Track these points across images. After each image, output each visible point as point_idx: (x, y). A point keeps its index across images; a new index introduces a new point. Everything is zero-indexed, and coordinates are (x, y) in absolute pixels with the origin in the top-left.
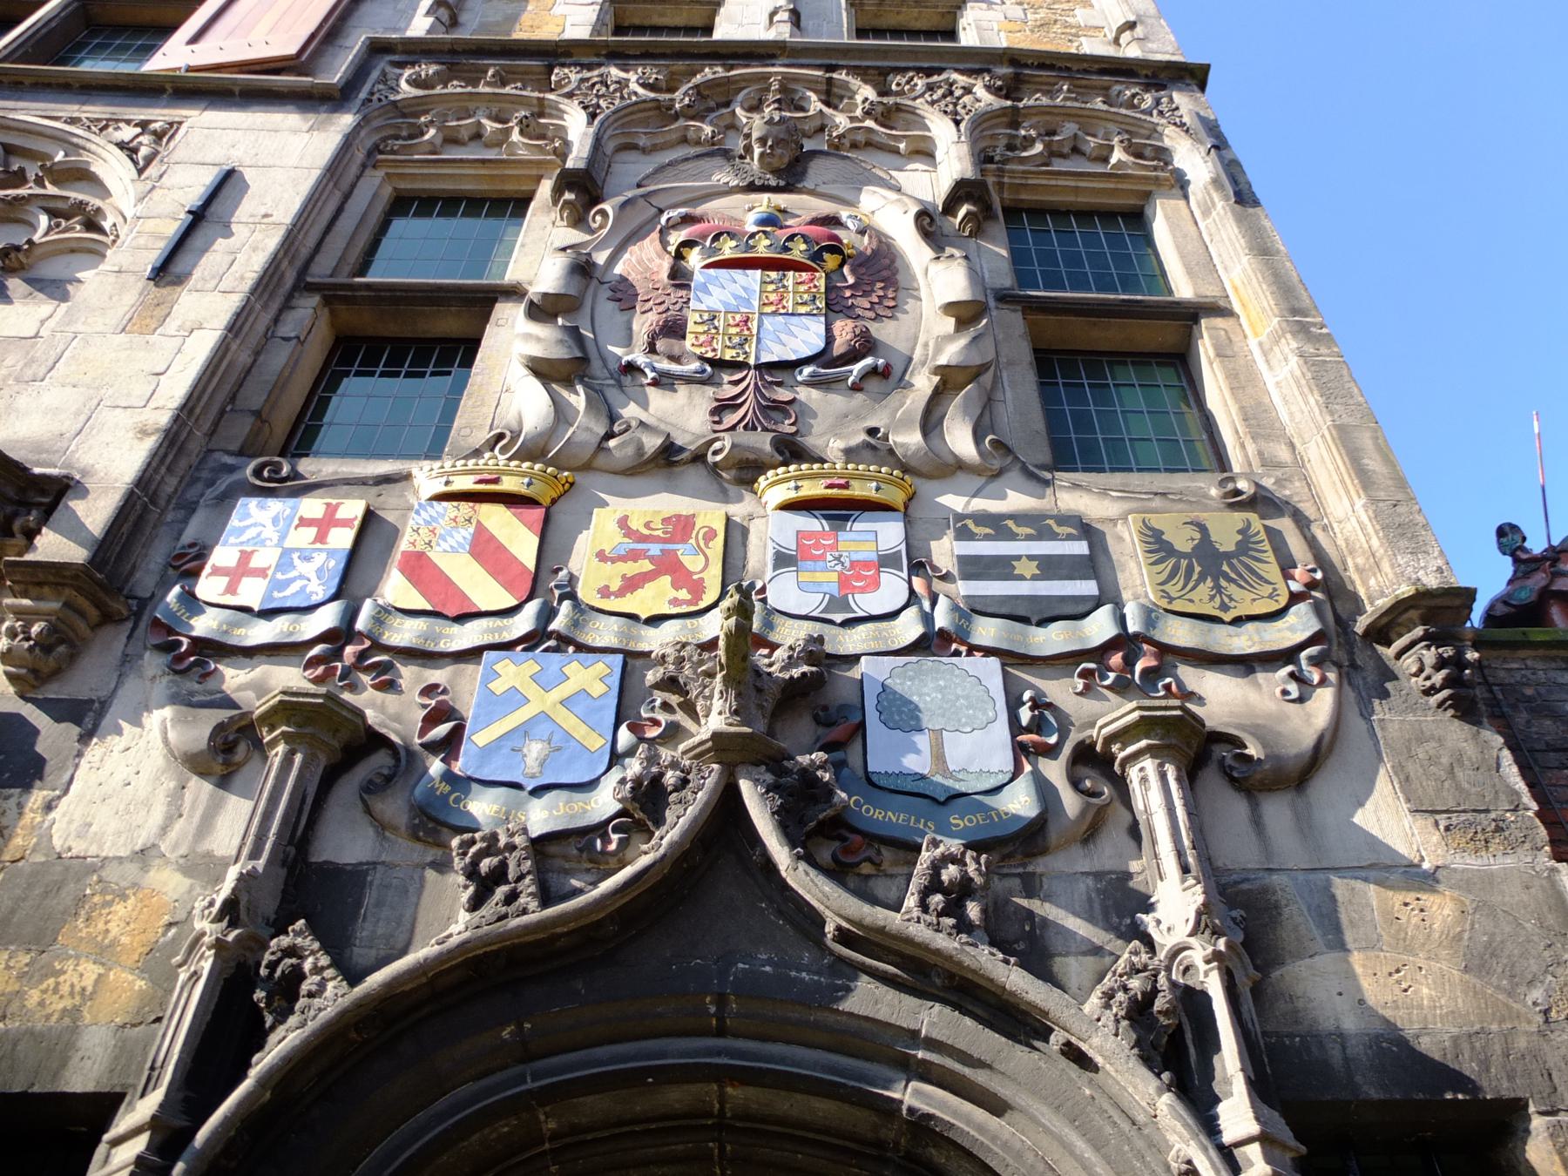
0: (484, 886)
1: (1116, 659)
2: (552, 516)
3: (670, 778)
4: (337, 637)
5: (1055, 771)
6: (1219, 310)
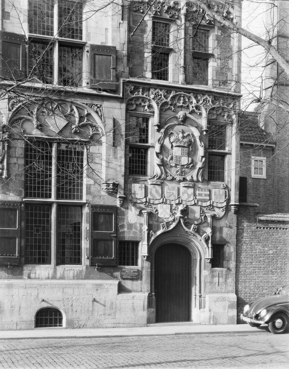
0: (163, 228)
1: (209, 207)
2: (161, 185)
3: (176, 219)
4: (146, 202)
5: (203, 217)
6: (230, 154)
